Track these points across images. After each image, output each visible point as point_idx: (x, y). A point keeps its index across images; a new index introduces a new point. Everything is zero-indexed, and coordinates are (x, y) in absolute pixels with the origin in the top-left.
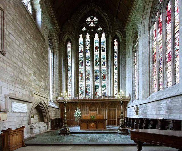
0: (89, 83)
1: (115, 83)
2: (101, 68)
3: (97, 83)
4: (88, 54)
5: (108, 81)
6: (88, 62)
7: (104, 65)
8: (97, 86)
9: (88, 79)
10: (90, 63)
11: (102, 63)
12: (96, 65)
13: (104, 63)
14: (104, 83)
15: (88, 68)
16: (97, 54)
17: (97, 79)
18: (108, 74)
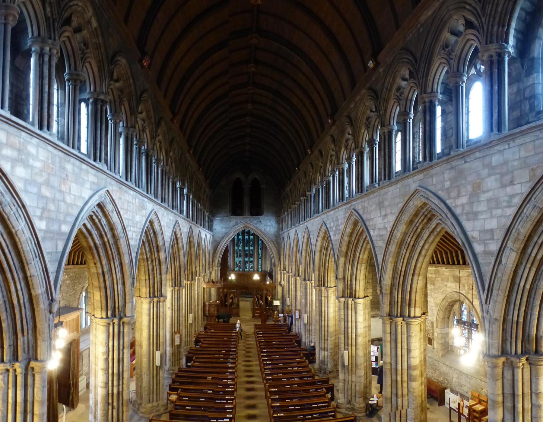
0: (241, 259)
1: (259, 260)
2: (249, 248)
3: (246, 259)
4: (240, 237)
5: (254, 258)
6: (240, 243)
7: (252, 246)
8: (247, 262)
9: (240, 256)
10: (241, 244)
11: (251, 244)
12: (247, 246)
13: (252, 244)
14: (251, 259)
15: (240, 248)
16: (247, 237)
17: (246, 257)
18: (254, 253)
